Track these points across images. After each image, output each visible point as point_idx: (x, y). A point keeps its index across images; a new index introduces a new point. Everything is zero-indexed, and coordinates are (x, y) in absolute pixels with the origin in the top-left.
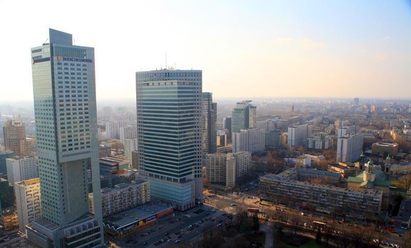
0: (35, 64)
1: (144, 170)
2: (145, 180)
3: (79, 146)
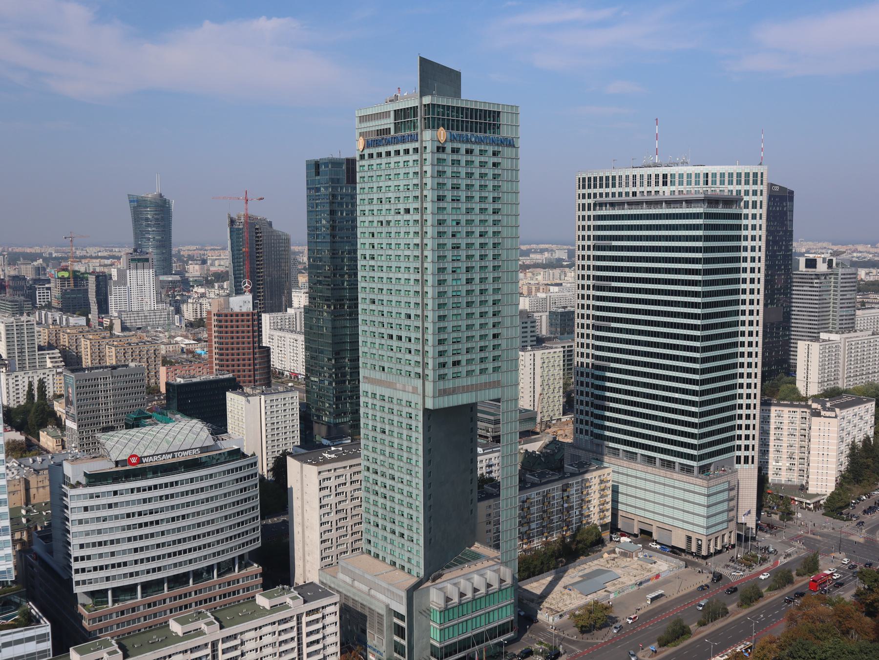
3: (477, 368)
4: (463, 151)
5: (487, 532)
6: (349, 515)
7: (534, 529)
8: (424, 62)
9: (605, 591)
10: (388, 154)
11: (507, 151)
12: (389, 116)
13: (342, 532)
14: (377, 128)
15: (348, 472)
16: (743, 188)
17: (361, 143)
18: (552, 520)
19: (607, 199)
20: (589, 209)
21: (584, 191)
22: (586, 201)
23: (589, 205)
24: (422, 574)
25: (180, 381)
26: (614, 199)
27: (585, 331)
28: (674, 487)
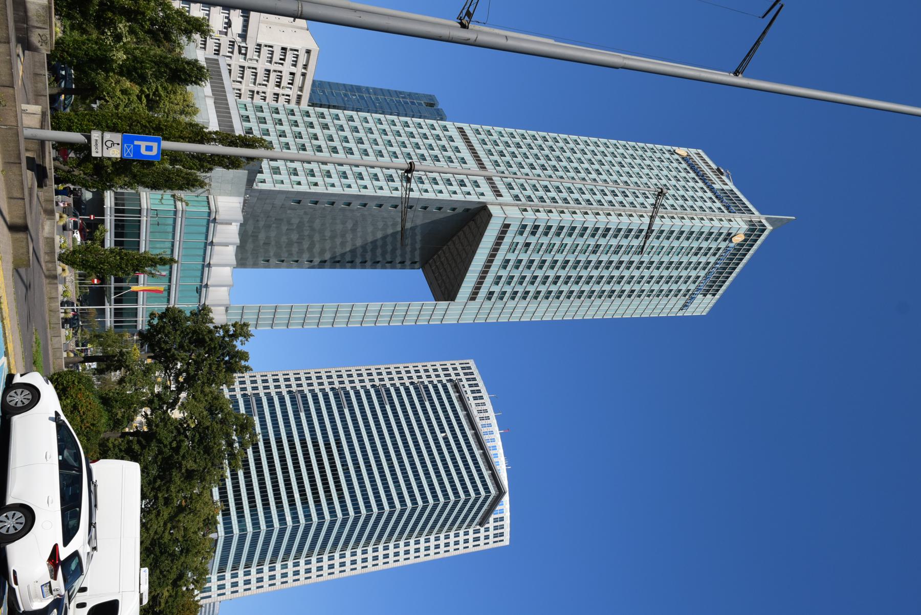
15: (293, 92)
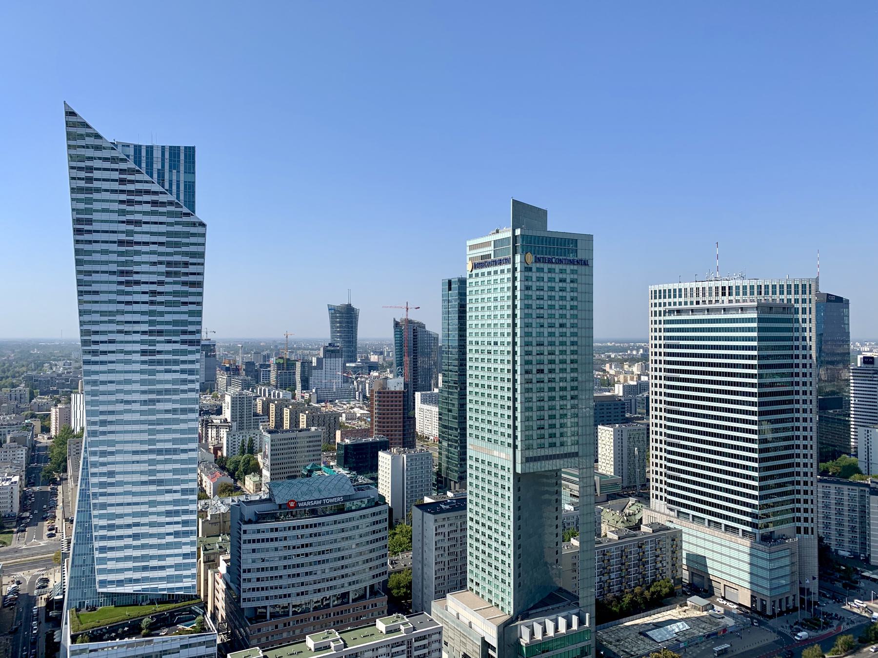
0: (474, 272)
1: (663, 502)
2: (668, 524)
4: (546, 270)
5: (573, 578)
6: (459, 557)
7: (614, 579)
8: (516, 203)
9: (676, 640)
10: (489, 273)
11: (581, 269)
12: (490, 245)
13: (453, 571)
14: (480, 254)
16: (792, 297)
17: (469, 266)
18: (630, 572)
19: (675, 307)
20: (660, 315)
21: (657, 301)
22: (657, 309)
23: (660, 312)
24: (512, 613)
25: (347, 441)
26: (680, 307)
27: (658, 413)
28: (739, 551)
